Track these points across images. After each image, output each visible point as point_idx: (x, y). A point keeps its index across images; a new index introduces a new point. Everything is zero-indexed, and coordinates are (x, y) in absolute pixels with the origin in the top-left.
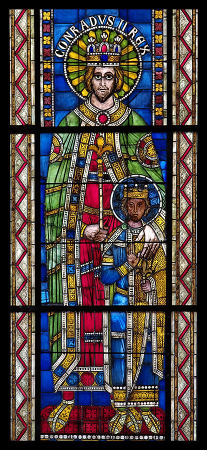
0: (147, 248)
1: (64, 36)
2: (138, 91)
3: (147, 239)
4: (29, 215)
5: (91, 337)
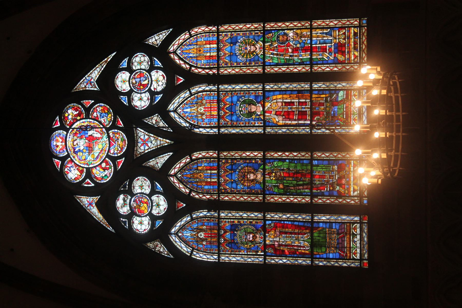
2: (254, 39)
4: (286, 67)
5: (319, 50)
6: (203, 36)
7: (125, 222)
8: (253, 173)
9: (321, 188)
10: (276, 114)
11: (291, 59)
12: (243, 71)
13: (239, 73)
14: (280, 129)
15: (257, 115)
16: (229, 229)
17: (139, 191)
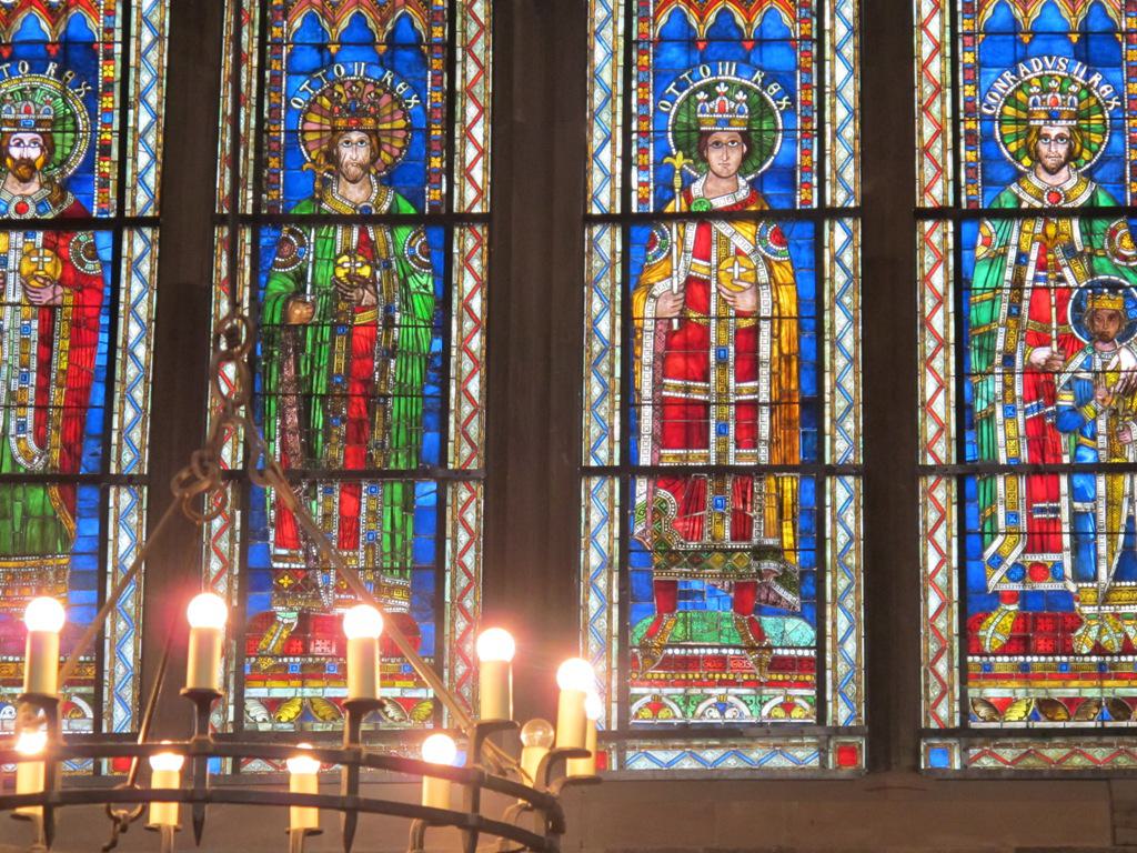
0: (1124, 380)
1: (995, 84)
3: (1124, 368)
4: (947, 334)
5: (1042, 510)
8: (374, 159)
9: (288, 529)
10: (691, 282)
11: (990, 362)
12: (931, 102)
13: (920, 77)
14: (608, 304)
15: (688, 181)
16: (72, 31)
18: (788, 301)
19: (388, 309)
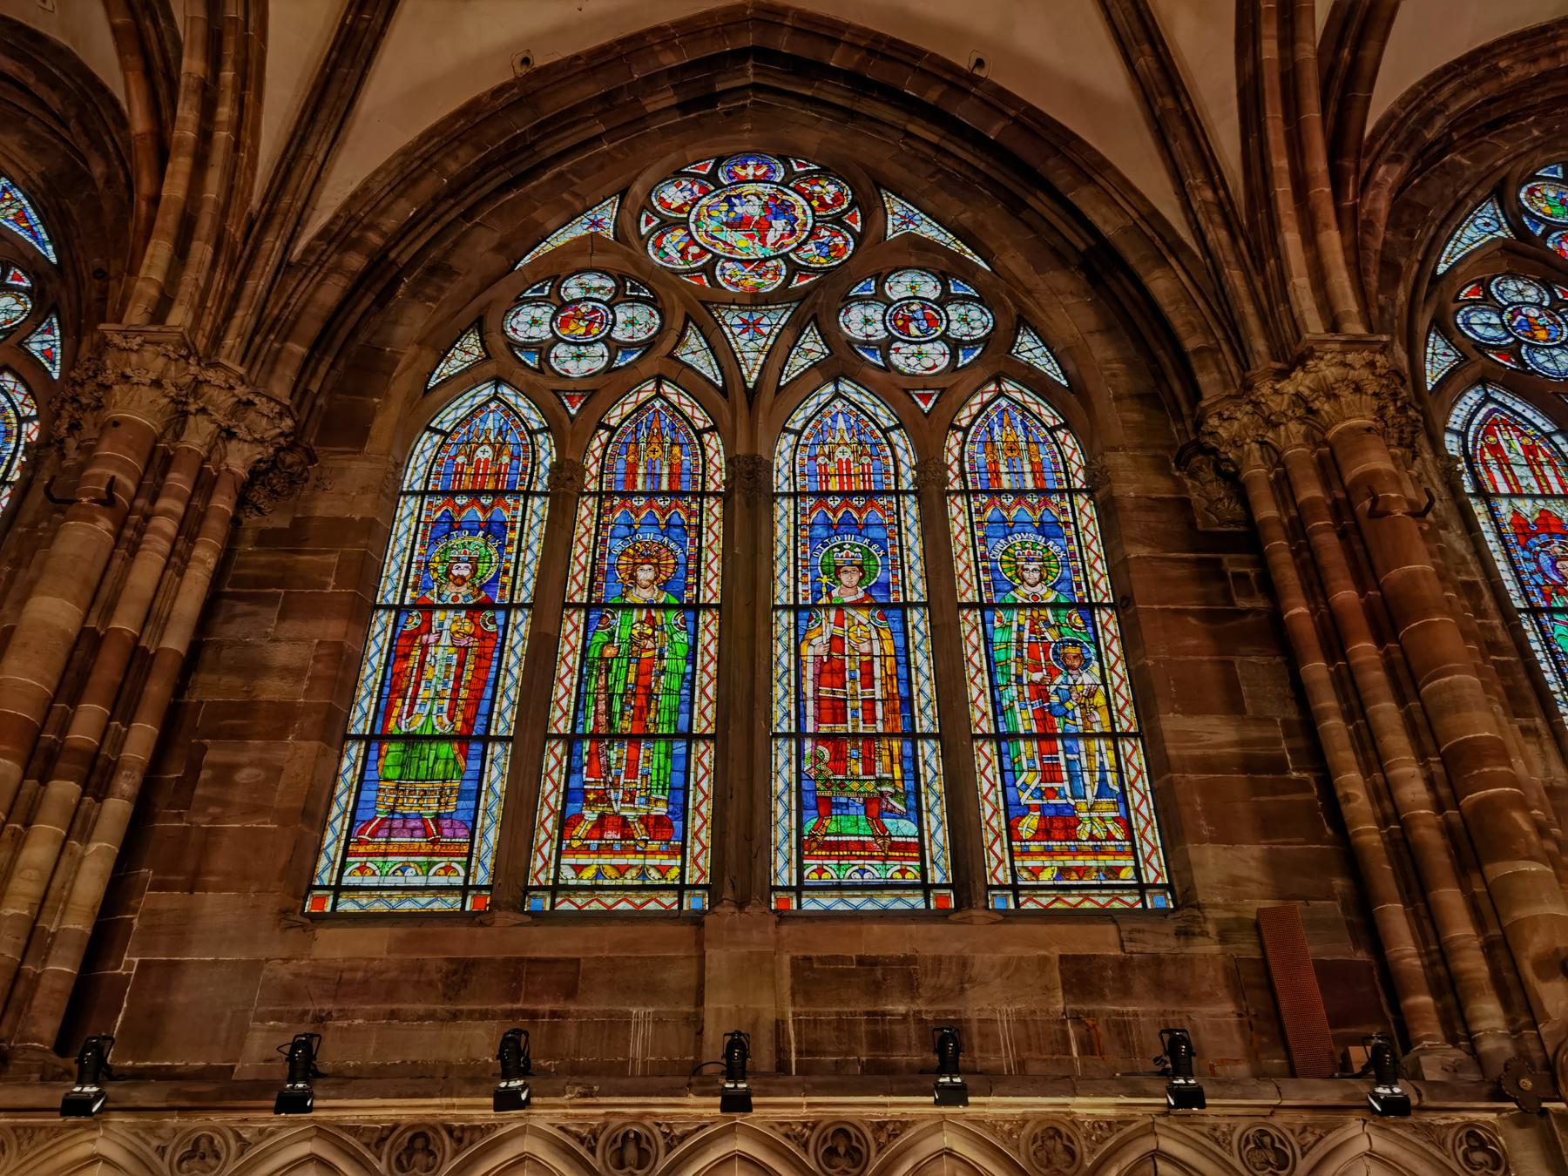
6: (1054, 457)
7: (541, 289)
9: (595, 767)
10: (833, 637)
15: (830, 589)
17: (621, 317)
18: (889, 650)
19: (661, 649)
